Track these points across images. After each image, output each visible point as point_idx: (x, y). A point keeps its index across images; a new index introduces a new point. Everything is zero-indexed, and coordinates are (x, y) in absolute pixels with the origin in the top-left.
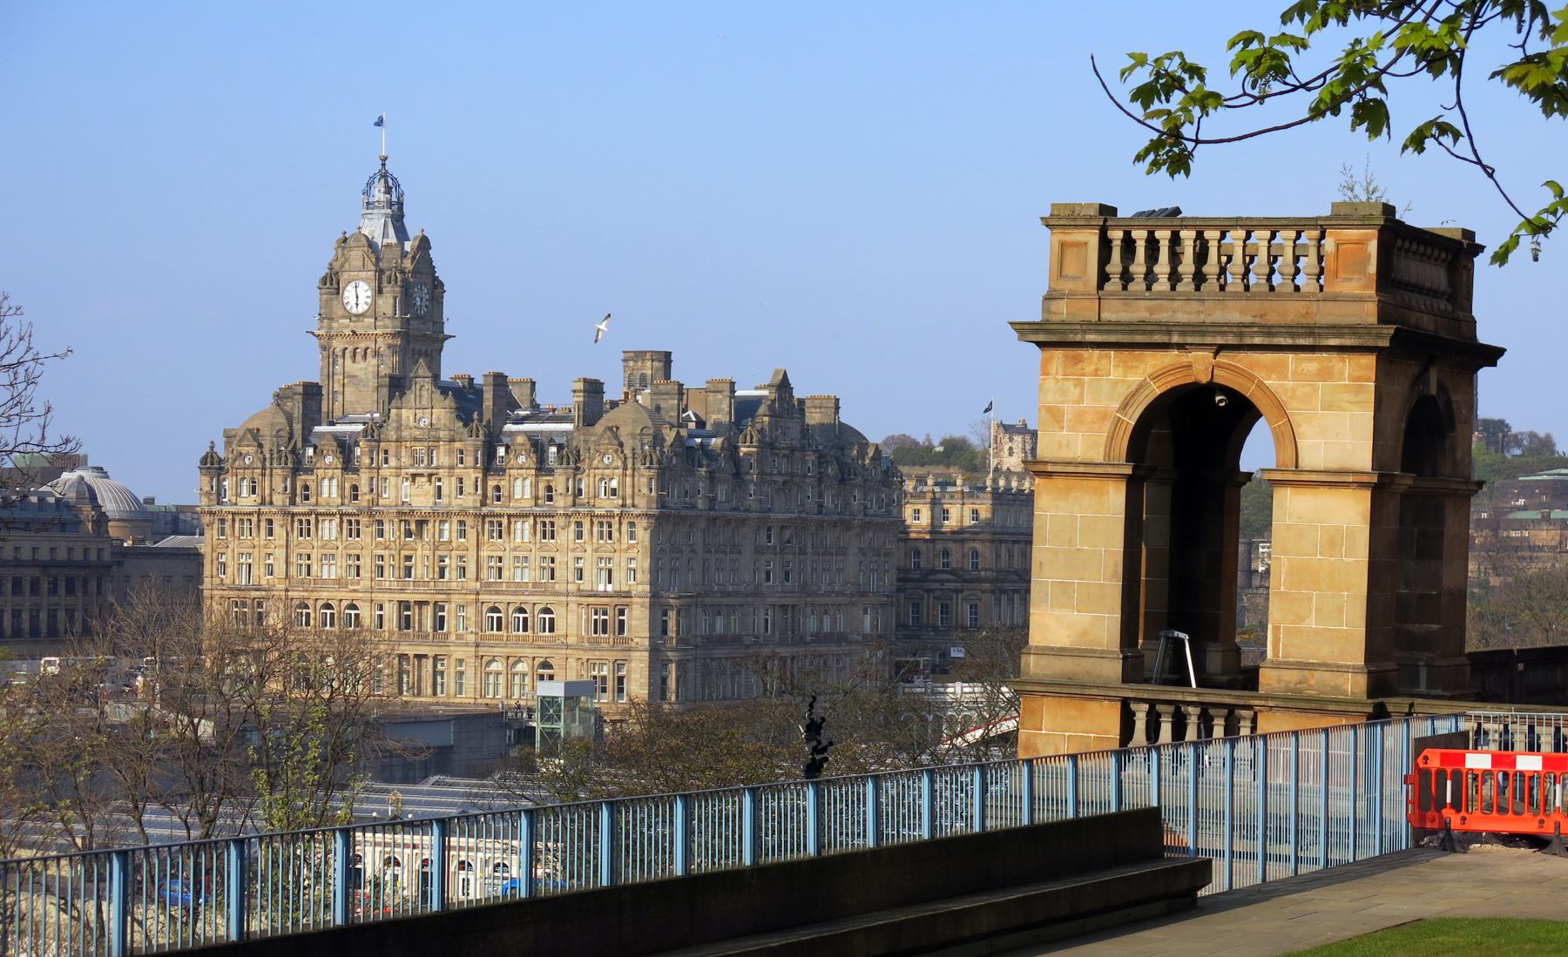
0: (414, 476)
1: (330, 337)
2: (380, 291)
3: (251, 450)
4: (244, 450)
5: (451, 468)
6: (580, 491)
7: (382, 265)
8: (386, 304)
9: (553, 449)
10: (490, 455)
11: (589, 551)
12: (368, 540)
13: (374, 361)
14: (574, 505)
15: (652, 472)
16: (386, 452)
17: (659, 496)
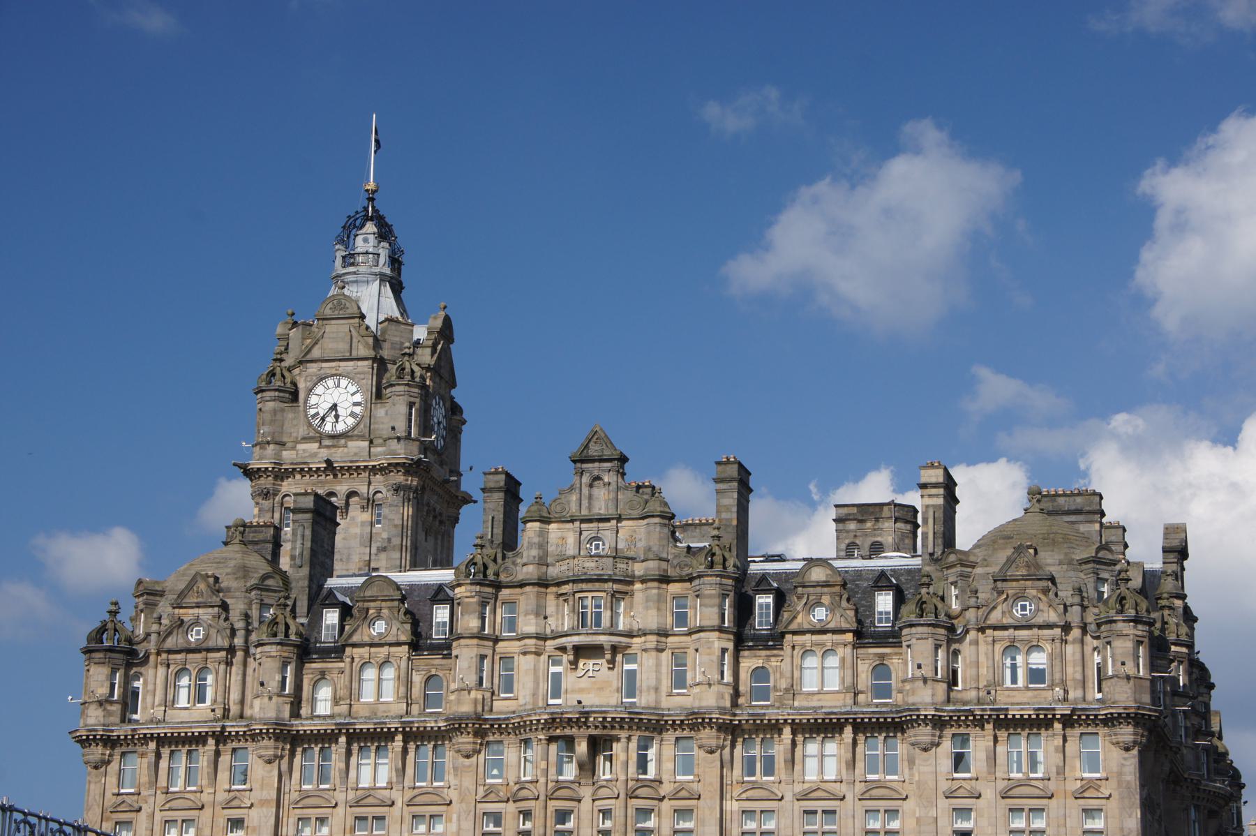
0: (581, 652)
1: (281, 474)
2: (379, 395)
3: (205, 614)
4: (188, 615)
5: (663, 633)
6: (955, 672)
7: (386, 353)
8: (396, 412)
9: (884, 602)
10: (744, 608)
11: (989, 793)
12: (468, 782)
13: (366, 516)
14: (949, 701)
15: (1141, 630)
16: (511, 604)
17: (1153, 681)
